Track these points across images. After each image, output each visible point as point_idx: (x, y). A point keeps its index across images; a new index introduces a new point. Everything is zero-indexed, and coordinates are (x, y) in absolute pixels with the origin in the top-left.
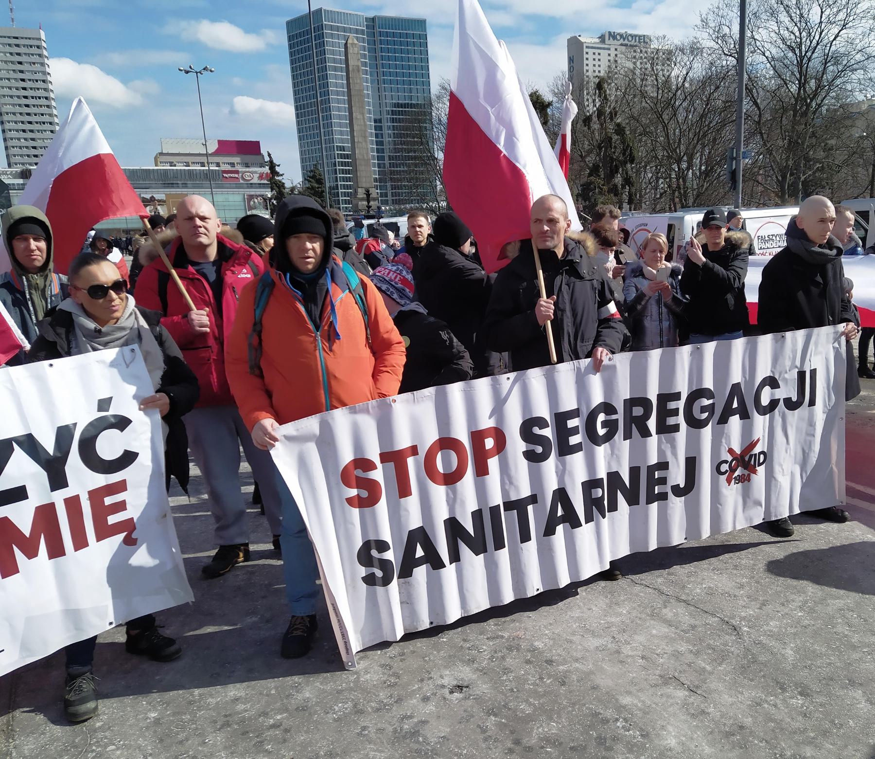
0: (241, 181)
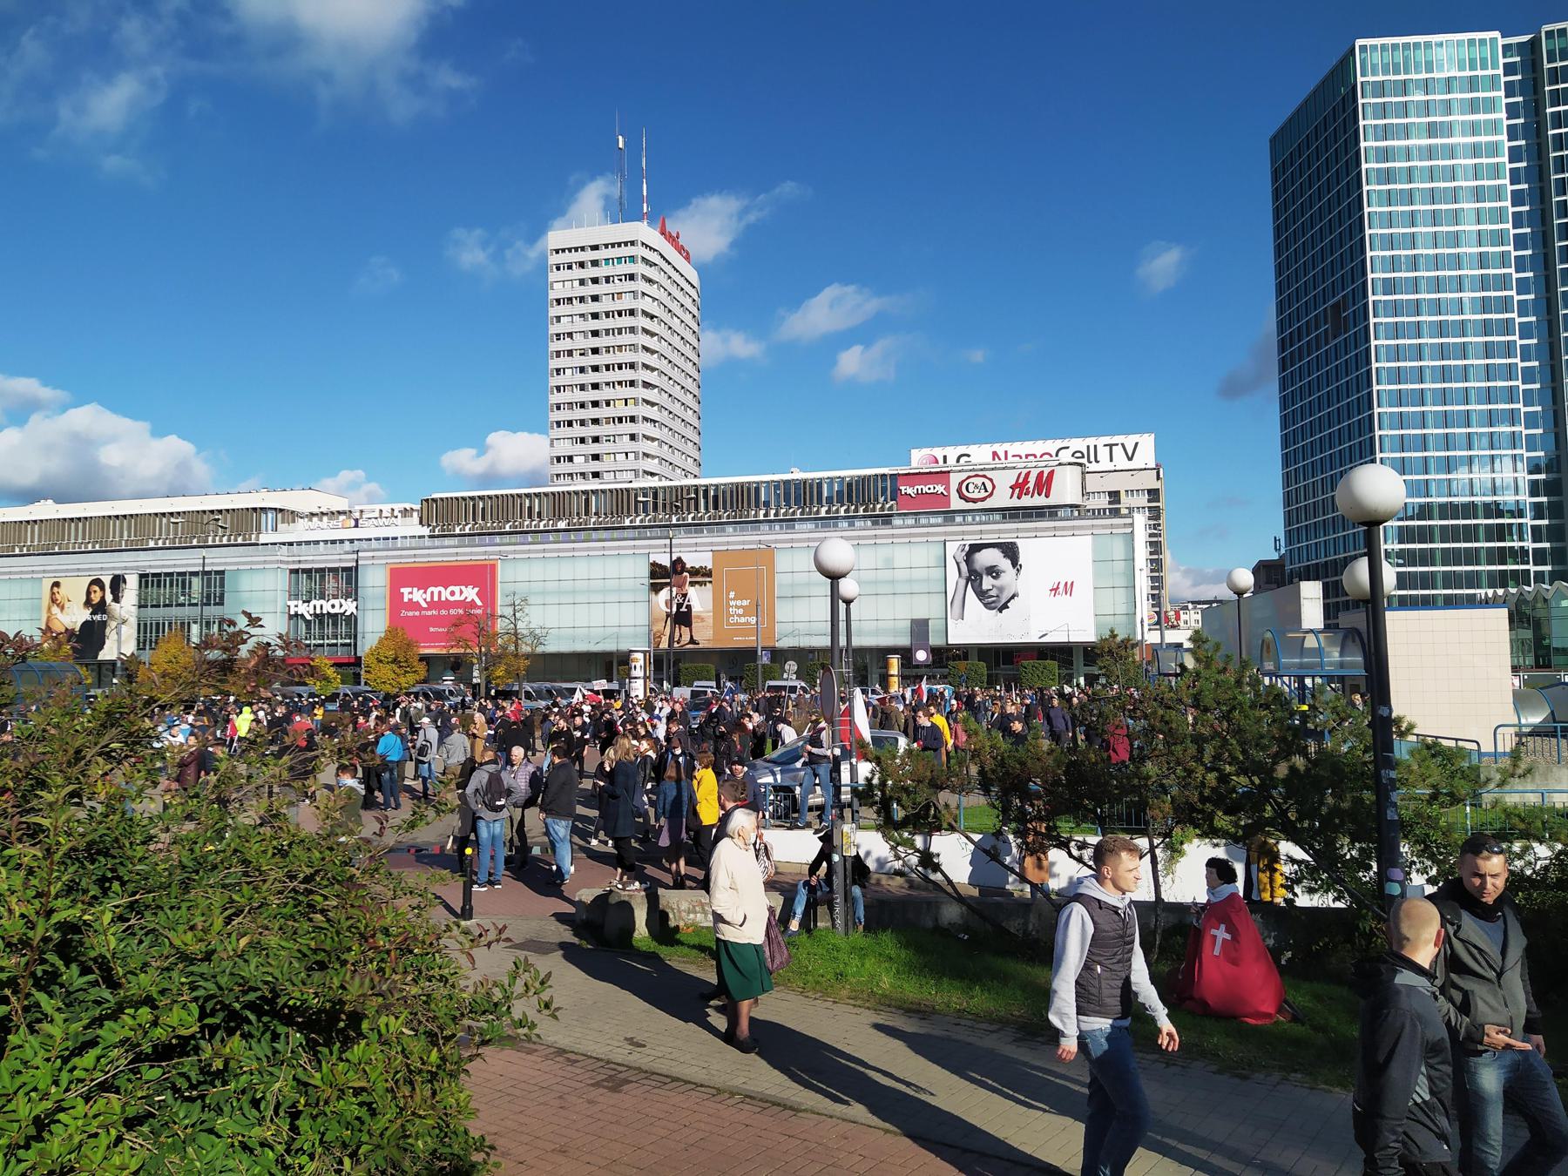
0: (956, 503)
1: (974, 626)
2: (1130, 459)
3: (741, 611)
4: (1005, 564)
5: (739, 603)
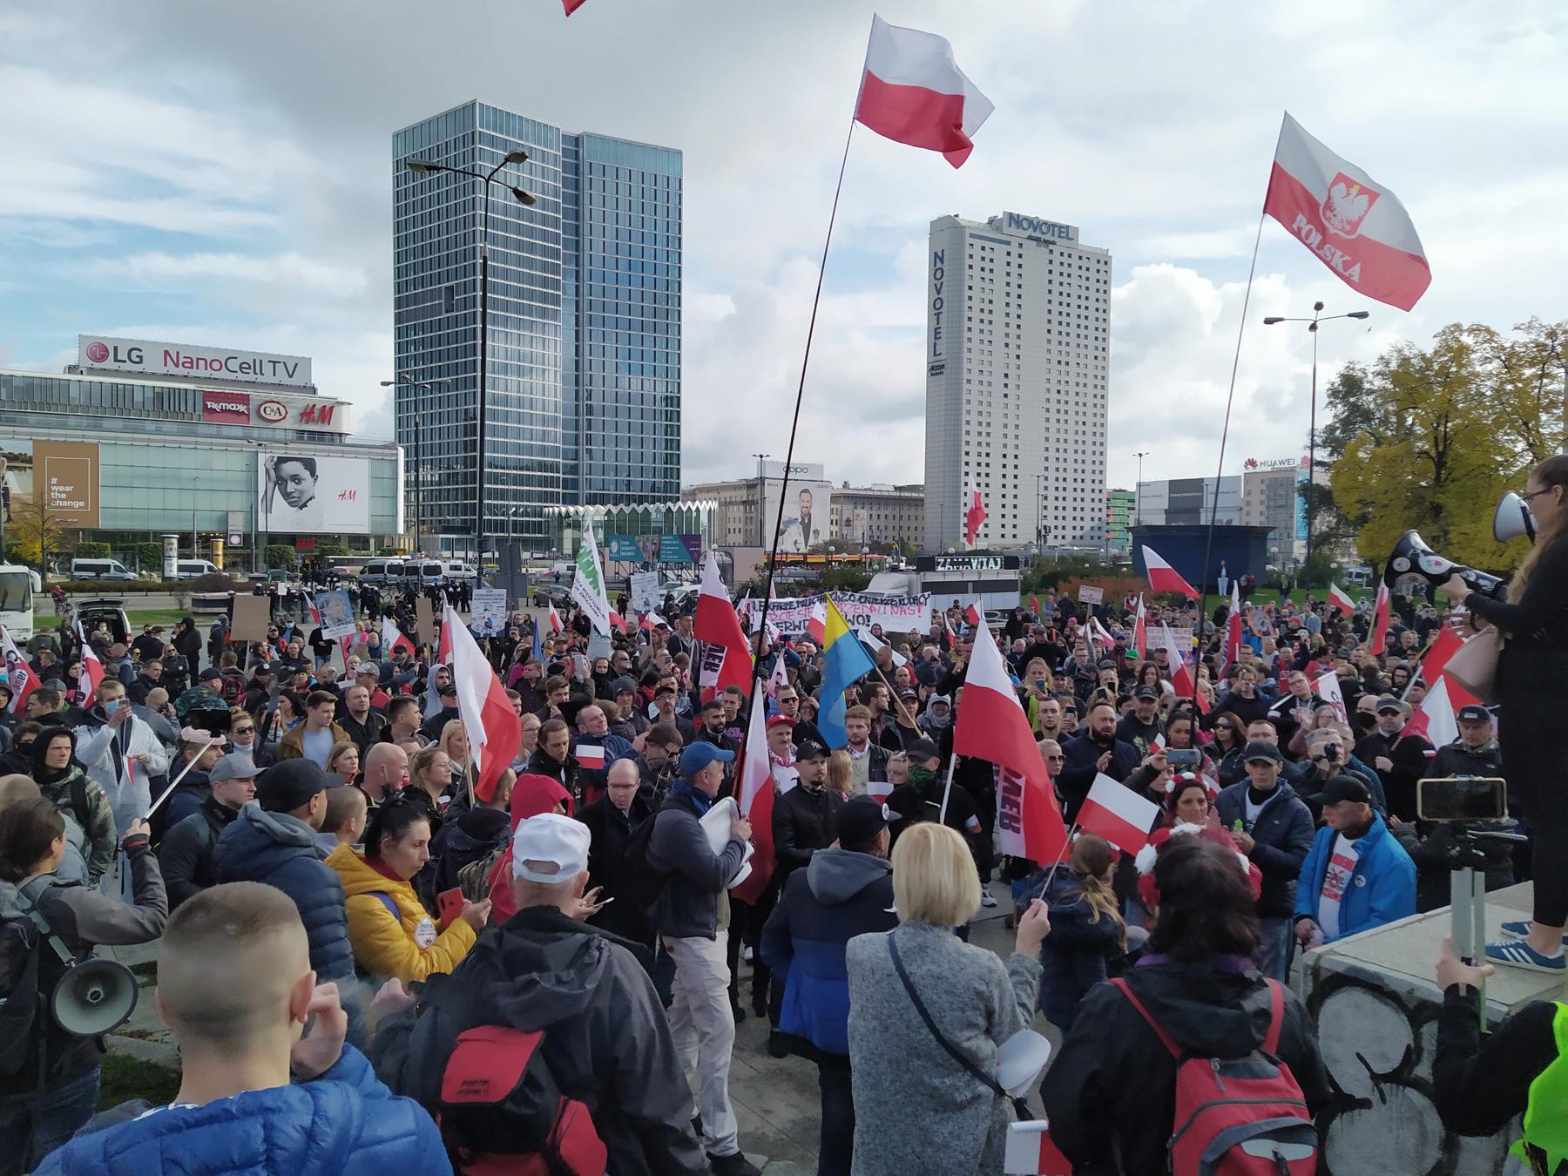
1: (281, 518)
2: (291, 376)
3: (64, 496)
4: (305, 474)
5: (61, 488)
